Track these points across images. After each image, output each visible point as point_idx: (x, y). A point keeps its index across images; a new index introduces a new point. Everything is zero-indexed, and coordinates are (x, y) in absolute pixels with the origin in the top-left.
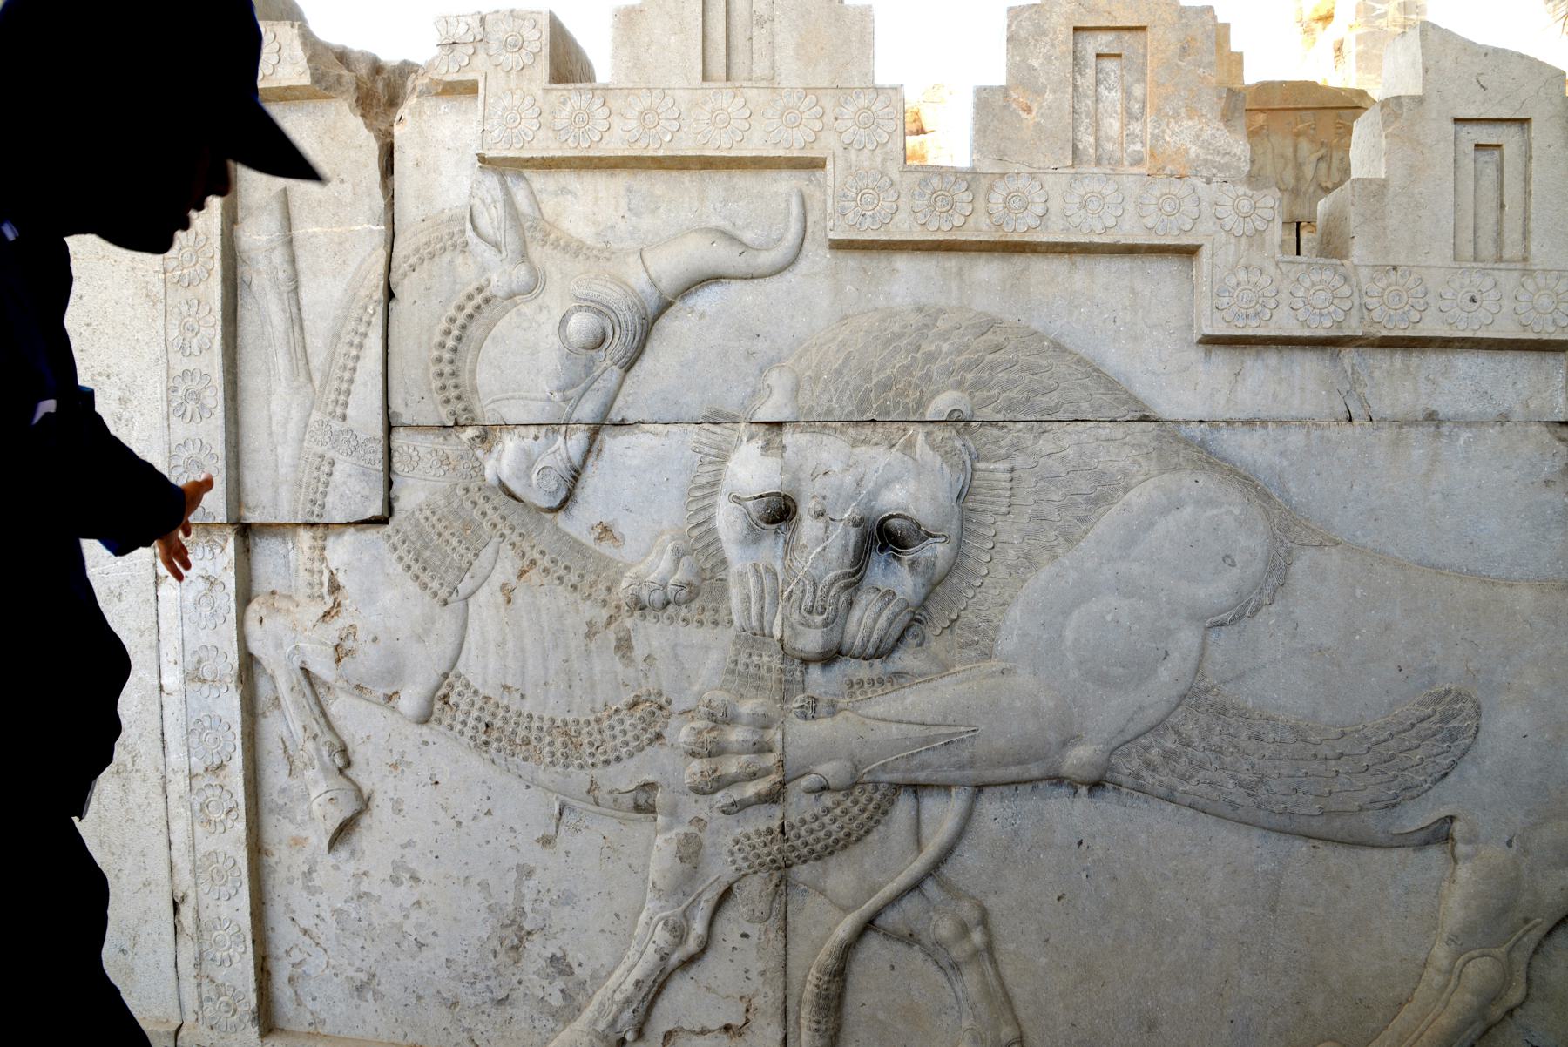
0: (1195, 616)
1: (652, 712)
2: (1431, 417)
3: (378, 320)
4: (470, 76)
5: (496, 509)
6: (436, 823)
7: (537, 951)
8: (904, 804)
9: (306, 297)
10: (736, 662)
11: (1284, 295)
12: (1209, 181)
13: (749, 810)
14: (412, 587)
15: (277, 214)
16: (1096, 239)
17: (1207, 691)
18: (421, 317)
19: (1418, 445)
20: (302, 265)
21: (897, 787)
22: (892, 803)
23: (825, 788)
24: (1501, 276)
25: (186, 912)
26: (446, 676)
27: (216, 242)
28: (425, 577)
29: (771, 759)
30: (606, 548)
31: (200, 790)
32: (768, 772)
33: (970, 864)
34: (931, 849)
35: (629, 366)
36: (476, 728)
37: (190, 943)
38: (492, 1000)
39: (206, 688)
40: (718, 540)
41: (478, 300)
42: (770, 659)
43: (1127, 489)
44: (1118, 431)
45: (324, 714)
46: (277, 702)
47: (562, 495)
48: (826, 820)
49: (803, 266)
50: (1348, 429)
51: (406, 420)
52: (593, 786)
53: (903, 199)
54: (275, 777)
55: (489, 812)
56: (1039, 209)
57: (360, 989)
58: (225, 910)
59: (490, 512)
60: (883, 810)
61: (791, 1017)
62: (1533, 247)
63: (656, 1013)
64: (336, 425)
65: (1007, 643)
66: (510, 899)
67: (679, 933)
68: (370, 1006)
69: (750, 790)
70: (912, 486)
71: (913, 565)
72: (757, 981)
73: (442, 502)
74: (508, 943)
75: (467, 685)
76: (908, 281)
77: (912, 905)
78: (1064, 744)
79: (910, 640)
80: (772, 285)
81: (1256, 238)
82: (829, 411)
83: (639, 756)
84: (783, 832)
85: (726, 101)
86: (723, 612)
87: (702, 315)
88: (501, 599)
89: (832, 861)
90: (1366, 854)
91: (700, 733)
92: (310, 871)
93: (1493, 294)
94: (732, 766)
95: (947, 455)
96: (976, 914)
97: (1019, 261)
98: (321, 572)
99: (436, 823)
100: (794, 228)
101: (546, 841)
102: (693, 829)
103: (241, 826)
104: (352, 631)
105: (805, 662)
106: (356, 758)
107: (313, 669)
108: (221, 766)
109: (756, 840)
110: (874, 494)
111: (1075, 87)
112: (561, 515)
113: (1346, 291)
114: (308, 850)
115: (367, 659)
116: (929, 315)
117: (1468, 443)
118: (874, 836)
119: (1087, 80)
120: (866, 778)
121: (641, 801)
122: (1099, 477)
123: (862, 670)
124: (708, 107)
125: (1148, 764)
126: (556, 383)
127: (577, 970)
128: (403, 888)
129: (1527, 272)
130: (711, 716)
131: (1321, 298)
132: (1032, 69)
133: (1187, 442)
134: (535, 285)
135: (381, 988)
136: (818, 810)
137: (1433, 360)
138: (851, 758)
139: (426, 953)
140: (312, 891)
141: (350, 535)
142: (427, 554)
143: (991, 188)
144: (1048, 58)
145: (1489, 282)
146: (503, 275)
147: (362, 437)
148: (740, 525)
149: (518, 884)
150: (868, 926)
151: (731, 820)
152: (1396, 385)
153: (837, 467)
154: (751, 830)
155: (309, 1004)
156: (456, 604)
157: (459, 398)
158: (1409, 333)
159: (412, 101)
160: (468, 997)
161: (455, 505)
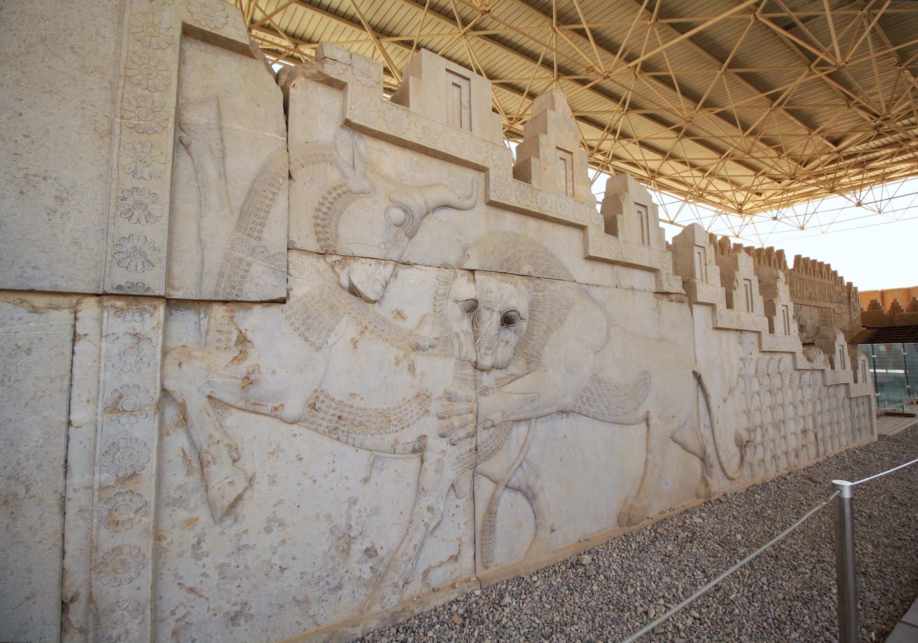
6: (299, 484)
7: (358, 548)
25: (77, 613)
29: (471, 417)
30: (399, 323)
35: (410, 238)
38: (329, 589)
39: (124, 419)
41: (339, 191)
42: (469, 370)
43: (574, 304)
48: (491, 441)
51: (298, 246)
52: (396, 441)
55: (334, 470)
57: (234, 619)
58: (126, 591)
61: (478, 542)
64: (254, 243)
71: (515, 332)
74: (341, 548)
75: (327, 396)
80: (465, 213)
82: (491, 267)
87: (440, 221)
88: (351, 346)
92: (199, 543)
94: (456, 422)
99: (299, 484)
101: (366, 480)
104: (256, 369)
107: (218, 395)
108: (134, 474)
114: (198, 528)
118: (506, 446)
121: (417, 447)
125: (583, 403)
127: (380, 552)
130: (450, 399)
135: (252, 611)
139: (287, 573)
141: (257, 307)
142: (311, 321)
146: (356, 183)
147: (272, 252)
149: (350, 507)
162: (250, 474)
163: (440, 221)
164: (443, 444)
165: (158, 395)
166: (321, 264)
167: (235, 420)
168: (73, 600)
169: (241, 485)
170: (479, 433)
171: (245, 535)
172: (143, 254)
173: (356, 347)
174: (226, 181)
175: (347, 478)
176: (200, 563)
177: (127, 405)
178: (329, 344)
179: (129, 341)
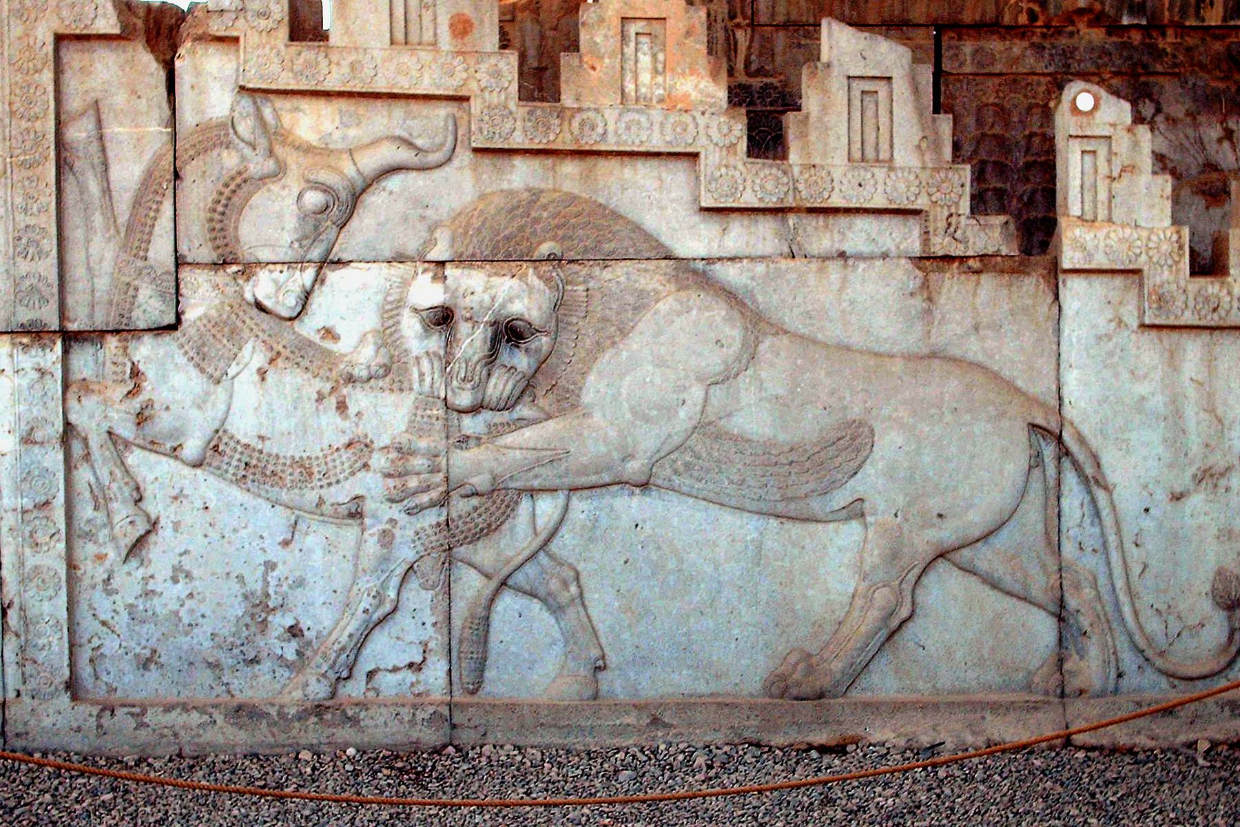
0: (699, 379)
1: (360, 446)
2: (842, 255)
3: (170, 193)
4: (235, 34)
5: (252, 318)
7: (280, 621)
8: (525, 505)
9: (115, 173)
10: (415, 415)
11: (748, 183)
12: (703, 113)
13: (426, 512)
14: (194, 372)
15: (93, 119)
16: (636, 149)
17: (710, 423)
18: (198, 192)
19: (834, 270)
20: (110, 154)
21: (520, 491)
22: (517, 503)
23: (476, 494)
24: (876, 171)
26: (217, 431)
27: (51, 137)
28: (203, 365)
30: (328, 345)
31: (29, 522)
32: (438, 486)
33: (566, 543)
34: (543, 536)
36: (237, 467)
37: (14, 638)
39: (36, 449)
40: (402, 336)
41: (238, 180)
42: (439, 411)
43: (657, 302)
44: (651, 265)
45: (123, 463)
46: (87, 457)
47: (299, 309)
48: (475, 515)
49: (456, 162)
50: (791, 263)
51: (189, 259)
52: (321, 502)
53: (518, 123)
54: (86, 511)
56: (600, 130)
58: (46, 607)
59: (248, 321)
60: (512, 507)
61: (454, 654)
62: (895, 154)
63: (361, 659)
64: (140, 263)
65: (588, 397)
66: (258, 587)
67: (379, 597)
68: (153, 675)
69: (425, 498)
70: (526, 301)
71: (527, 350)
72: (430, 630)
73: (216, 315)
75: (232, 438)
76: (522, 174)
77: (530, 569)
78: (623, 460)
79: (527, 399)
80: (436, 174)
81: (731, 147)
82: (473, 255)
83: (351, 479)
84: (448, 525)
85: (406, 59)
86: (406, 385)
88: (257, 378)
89: (480, 544)
90: (812, 527)
91: (393, 461)
92: (109, 579)
93: (872, 182)
94: (413, 483)
95: (548, 280)
96: (572, 573)
97: (590, 161)
98: (125, 365)
100: (450, 139)
101: (286, 543)
102: (388, 526)
103: (61, 546)
104: (149, 404)
105: (460, 412)
106: (148, 494)
108: (47, 503)
109: (429, 531)
110: (503, 306)
111: (623, 54)
112: (296, 322)
113: (785, 180)
114: (107, 563)
115: (163, 422)
116: (535, 194)
117: (863, 270)
118: (506, 526)
119: (630, 50)
120: (501, 486)
121: (353, 510)
122: (641, 293)
123: (500, 417)
124: (395, 61)
125: (676, 472)
126: (296, 236)
127: (306, 633)
128: (179, 586)
129: (891, 169)
130: (399, 450)
131: (769, 186)
132: (596, 44)
133: (695, 272)
134: (279, 172)
135: (162, 660)
136: (469, 508)
137: (843, 221)
138: (491, 472)
140: (109, 593)
141: (147, 338)
142: (206, 349)
143: (573, 116)
144: (606, 36)
145: (869, 175)
146: (258, 165)
148: (418, 327)
149: (266, 574)
150: (504, 583)
151: (413, 519)
152: (822, 237)
153: (479, 289)
154: (426, 525)
155: (105, 678)
156: (225, 382)
157: (226, 245)
158: (823, 205)
159: (188, 44)
160: (227, 660)
161: (225, 316)
162: (153, 517)
163: (391, 193)
164: (395, 512)
165: (61, 429)
166: (221, 277)
167: (135, 458)
168: (9, 607)
169: (141, 528)
170: (453, 503)
171: (151, 581)
172: (40, 292)
173: (263, 379)
174: (111, 198)
175: (261, 537)
176: (112, 599)
177: (38, 435)
178: (230, 376)
179: (36, 375)
